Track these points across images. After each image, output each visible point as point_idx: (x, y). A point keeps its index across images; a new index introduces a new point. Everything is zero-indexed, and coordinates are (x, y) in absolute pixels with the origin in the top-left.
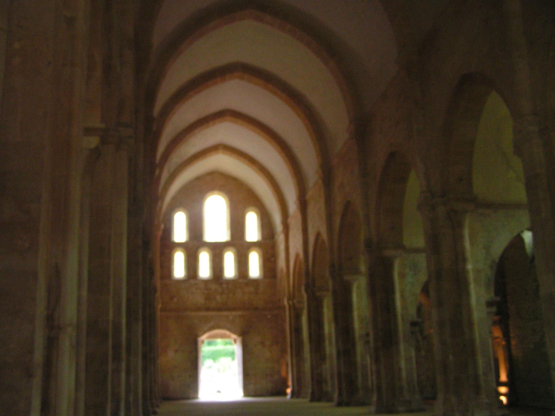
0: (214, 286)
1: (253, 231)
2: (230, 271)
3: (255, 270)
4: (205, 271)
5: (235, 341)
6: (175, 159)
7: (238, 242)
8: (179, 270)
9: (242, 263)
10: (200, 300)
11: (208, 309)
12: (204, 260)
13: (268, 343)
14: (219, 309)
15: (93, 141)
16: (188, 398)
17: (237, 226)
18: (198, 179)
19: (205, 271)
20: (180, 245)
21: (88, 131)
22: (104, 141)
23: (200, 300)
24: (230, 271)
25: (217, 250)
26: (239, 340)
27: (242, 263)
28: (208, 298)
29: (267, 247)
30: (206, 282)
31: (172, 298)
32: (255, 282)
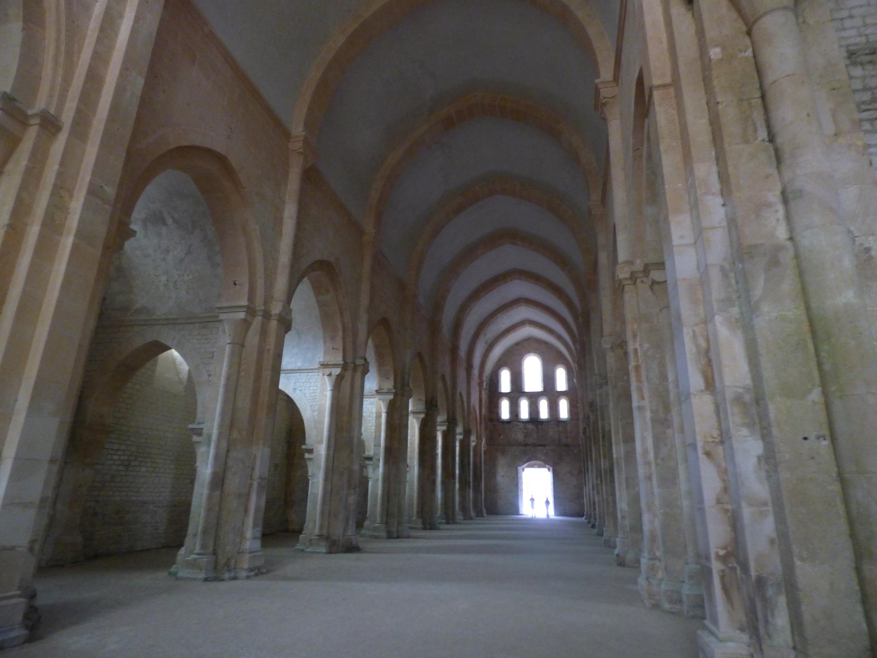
0: (530, 426)
1: (561, 381)
2: (544, 414)
4: (524, 413)
7: (549, 391)
8: (505, 413)
9: (554, 408)
10: (520, 436)
11: (526, 445)
14: (535, 445)
15: (337, 371)
17: (549, 379)
18: (517, 344)
19: (524, 413)
20: (506, 395)
23: (520, 436)
24: (544, 414)
25: (533, 398)
27: (554, 408)
28: (527, 435)
30: (525, 422)
31: (500, 435)
32: (564, 422)
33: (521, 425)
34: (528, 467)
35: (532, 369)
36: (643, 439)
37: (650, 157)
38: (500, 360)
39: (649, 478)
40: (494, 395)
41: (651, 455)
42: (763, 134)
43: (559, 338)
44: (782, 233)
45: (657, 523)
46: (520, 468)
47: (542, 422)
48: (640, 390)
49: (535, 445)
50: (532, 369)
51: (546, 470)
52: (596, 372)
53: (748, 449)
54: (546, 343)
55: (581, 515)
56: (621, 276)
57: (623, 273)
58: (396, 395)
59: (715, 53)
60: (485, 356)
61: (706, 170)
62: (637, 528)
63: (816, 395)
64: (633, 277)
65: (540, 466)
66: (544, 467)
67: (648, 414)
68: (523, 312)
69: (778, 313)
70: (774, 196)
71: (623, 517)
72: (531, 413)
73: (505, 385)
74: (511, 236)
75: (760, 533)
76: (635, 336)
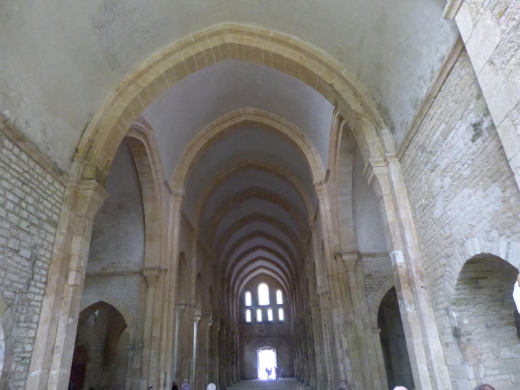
0: (263, 326)
1: (280, 300)
2: (270, 318)
4: (259, 318)
5: (274, 351)
6: (242, 276)
8: (248, 319)
9: (276, 314)
10: (257, 332)
12: (259, 313)
14: (266, 337)
15: (199, 318)
16: (254, 379)
17: (273, 297)
18: (255, 277)
19: (259, 318)
21: (198, 316)
22: (202, 317)
24: (270, 318)
25: (264, 309)
26: (275, 350)
27: (276, 314)
29: (286, 306)
30: (260, 323)
33: (258, 325)
34: (263, 350)
35: (263, 290)
36: (327, 349)
39: (329, 362)
41: (330, 355)
42: (349, 297)
43: (279, 276)
44: (352, 319)
45: (333, 376)
46: (258, 351)
47: (270, 323)
48: (326, 333)
49: (266, 337)
50: (263, 290)
51: (272, 351)
52: (305, 309)
53: (347, 361)
54: (271, 276)
55: (292, 376)
56: (319, 293)
57: (319, 292)
58: (213, 323)
59: (341, 276)
61: (339, 301)
62: (325, 380)
63: (357, 351)
64: (323, 294)
65: (269, 349)
66: (271, 349)
67: (329, 342)
68: (261, 263)
69: (351, 335)
70: (351, 311)
71: (320, 376)
72: (263, 318)
73: (248, 301)
74: (262, 234)
75: (350, 376)
76: (324, 314)
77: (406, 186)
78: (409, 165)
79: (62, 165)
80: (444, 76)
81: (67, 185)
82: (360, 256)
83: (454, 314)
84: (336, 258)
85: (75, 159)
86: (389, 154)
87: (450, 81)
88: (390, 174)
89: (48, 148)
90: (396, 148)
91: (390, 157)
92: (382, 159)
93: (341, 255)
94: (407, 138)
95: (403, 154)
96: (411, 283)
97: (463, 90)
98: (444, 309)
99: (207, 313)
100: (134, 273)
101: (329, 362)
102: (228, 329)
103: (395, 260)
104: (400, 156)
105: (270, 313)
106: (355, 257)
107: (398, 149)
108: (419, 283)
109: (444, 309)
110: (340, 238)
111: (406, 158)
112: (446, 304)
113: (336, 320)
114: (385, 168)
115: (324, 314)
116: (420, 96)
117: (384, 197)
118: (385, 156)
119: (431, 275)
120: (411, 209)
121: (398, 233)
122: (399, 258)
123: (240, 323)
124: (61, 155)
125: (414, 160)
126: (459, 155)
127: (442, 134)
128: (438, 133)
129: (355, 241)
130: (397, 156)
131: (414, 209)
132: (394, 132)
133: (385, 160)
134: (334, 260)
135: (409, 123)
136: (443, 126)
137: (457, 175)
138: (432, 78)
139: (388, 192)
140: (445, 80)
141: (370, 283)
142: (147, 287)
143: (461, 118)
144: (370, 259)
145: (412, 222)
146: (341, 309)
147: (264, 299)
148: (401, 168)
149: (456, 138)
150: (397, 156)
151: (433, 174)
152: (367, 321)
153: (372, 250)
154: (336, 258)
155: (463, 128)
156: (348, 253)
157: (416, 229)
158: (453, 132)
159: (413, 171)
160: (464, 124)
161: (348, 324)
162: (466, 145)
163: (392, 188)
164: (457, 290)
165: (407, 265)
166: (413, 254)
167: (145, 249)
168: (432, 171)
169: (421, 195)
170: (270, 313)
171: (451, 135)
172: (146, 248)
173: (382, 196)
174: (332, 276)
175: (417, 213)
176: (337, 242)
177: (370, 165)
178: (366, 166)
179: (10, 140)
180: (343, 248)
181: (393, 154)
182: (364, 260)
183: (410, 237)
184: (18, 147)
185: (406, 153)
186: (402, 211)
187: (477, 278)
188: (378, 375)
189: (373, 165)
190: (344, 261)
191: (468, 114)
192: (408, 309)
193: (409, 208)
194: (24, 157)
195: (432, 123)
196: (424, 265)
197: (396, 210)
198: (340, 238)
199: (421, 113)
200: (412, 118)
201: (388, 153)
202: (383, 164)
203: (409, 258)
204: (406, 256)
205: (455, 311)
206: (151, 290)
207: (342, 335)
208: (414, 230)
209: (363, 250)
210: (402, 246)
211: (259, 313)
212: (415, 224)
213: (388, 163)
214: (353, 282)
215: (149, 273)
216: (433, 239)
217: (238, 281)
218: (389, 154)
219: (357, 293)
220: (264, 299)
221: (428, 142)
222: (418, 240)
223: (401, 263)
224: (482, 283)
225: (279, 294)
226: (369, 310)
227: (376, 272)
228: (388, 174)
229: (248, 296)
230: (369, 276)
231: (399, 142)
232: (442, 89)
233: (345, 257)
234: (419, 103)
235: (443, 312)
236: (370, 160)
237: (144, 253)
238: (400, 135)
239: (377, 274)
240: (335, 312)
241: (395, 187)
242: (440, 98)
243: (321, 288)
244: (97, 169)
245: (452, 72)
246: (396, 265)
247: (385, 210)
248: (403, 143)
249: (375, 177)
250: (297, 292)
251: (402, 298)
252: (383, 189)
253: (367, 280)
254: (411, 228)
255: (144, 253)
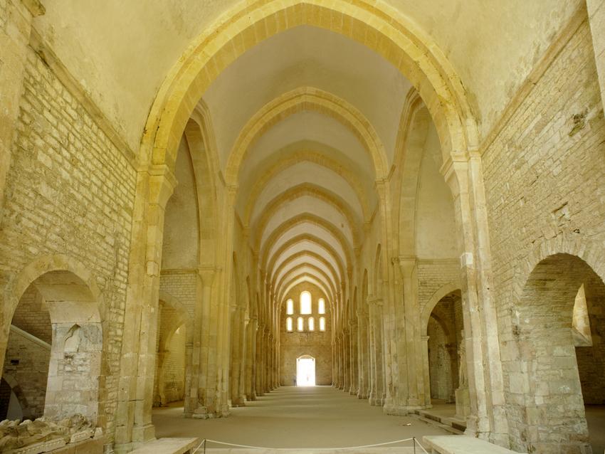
0: (304, 335)
1: (322, 310)
2: (311, 328)
3: (322, 327)
4: (300, 328)
6: (285, 282)
8: (289, 327)
9: (317, 324)
12: (300, 321)
13: (327, 361)
15: (246, 323)
17: (315, 307)
18: (298, 285)
19: (300, 328)
23: (298, 341)
24: (311, 328)
25: (306, 317)
27: (317, 324)
28: (302, 340)
29: (328, 316)
32: (322, 332)
35: (306, 299)
37: (381, 264)
38: (287, 294)
40: (284, 316)
43: (323, 284)
47: (310, 332)
48: (373, 340)
49: (306, 346)
50: (306, 299)
54: (314, 285)
57: (368, 300)
59: (396, 282)
60: (282, 294)
61: (392, 308)
68: (305, 270)
71: (361, 381)
72: (304, 328)
73: (290, 311)
77: (485, 185)
78: (492, 160)
79: (133, 146)
80: (551, 58)
81: (138, 170)
82: (417, 260)
83: (518, 314)
84: (393, 264)
85: (144, 141)
86: (472, 148)
87: (557, 63)
88: (470, 171)
89: (120, 126)
90: (480, 142)
91: (472, 151)
92: (463, 153)
93: (398, 261)
94: (494, 130)
95: (487, 149)
96: (478, 286)
97: (571, 75)
98: (508, 309)
99: (255, 318)
100: (189, 271)
101: (374, 368)
102: (271, 336)
103: (464, 261)
104: (483, 150)
105: (311, 321)
106: (413, 262)
107: (482, 143)
108: (486, 285)
109: (508, 309)
110: (399, 243)
111: (489, 153)
112: (511, 304)
113: (386, 326)
114: (466, 163)
115: (372, 322)
116: (517, 82)
117: (461, 196)
118: (467, 149)
119: (499, 277)
120: (488, 209)
121: (471, 235)
122: (470, 261)
123: (281, 331)
124: (131, 135)
125: (499, 155)
126: (552, 151)
127: (535, 128)
128: (532, 125)
129: (413, 247)
130: (479, 151)
131: (490, 210)
132: (479, 124)
133: (467, 154)
134: (390, 265)
135: (499, 114)
136: (540, 116)
137: (546, 173)
138: (535, 60)
139: (466, 191)
140: (551, 63)
141: (424, 291)
142: (203, 286)
143: (563, 109)
144: (427, 266)
145: (487, 223)
146: (394, 315)
147: (306, 308)
148: (483, 165)
149: (551, 132)
150: (479, 151)
151: (518, 171)
152: (418, 328)
153: (430, 257)
154: (393, 264)
155: (562, 120)
156: (407, 258)
157: (490, 231)
158: (550, 124)
159: (496, 168)
160: (564, 116)
161: (400, 330)
162: (561, 139)
163: (470, 186)
164: (524, 290)
165: (476, 267)
166: (483, 256)
167: (199, 247)
168: (518, 168)
169: (501, 194)
170: (311, 321)
171: (546, 129)
172: (201, 246)
173: (459, 195)
174: (388, 282)
175: (494, 214)
176: (395, 247)
177: (450, 159)
178: (445, 161)
179: (89, 115)
180: (401, 253)
181: (475, 148)
182: (420, 266)
183: (483, 238)
184: (96, 124)
185: (490, 147)
186: (478, 211)
187: (546, 280)
188: (422, 379)
189: (453, 159)
190: (400, 267)
191: (571, 105)
192: (472, 310)
193: (485, 208)
194: (101, 135)
195: (527, 113)
196: (492, 267)
197: (472, 209)
198: (399, 243)
199: (516, 101)
200: (503, 108)
201: (470, 146)
202: (464, 159)
203: (479, 260)
204: (477, 258)
205: (518, 311)
206: (207, 289)
207: (392, 341)
208: (488, 232)
209: (420, 255)
210: (473, 248)
211: (300, 321)
212: (489, 225)
213: (470, 158)
214: (408, 288)
215: (205, 272)
216: (507, 241)
217: (281, 288)
218: (472, 148)
219: (411, 300)
220: (306, 308)
221: (518, 135)
222: (491, 242)
223: (471, 265)
224: (550, 285)
225: (321, 303)
226: (421, 317)
227: (431, 279)
228: (468, 171)
229: (290, 304)
230: (423, 284)
231: (484, 135)
232: (545, 74)
233: (403, 263)
234: (515, 90)
235: (506, 312)
236: (452, 153)
237: (199, 252)
238: (487, 127)
239: (432, 282)
240: (387, 319)
241: (474, 184)
242: (542, 85)
243: (372, 295)
244: (167, 153)
245: (562, 53)
246: (465, 267)
247: (461, 211)
248: (489, 136)
249: (454, 174)
250: (342, 301)
251: (467, 299)
252: (461, 186)
253: (422, 288)
254: (485, 229)
255: (199, 252)
